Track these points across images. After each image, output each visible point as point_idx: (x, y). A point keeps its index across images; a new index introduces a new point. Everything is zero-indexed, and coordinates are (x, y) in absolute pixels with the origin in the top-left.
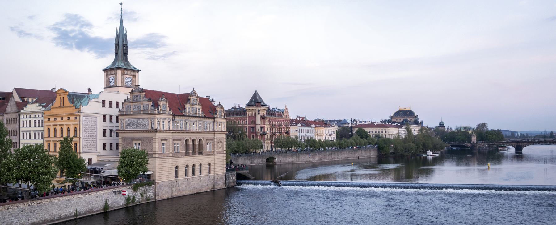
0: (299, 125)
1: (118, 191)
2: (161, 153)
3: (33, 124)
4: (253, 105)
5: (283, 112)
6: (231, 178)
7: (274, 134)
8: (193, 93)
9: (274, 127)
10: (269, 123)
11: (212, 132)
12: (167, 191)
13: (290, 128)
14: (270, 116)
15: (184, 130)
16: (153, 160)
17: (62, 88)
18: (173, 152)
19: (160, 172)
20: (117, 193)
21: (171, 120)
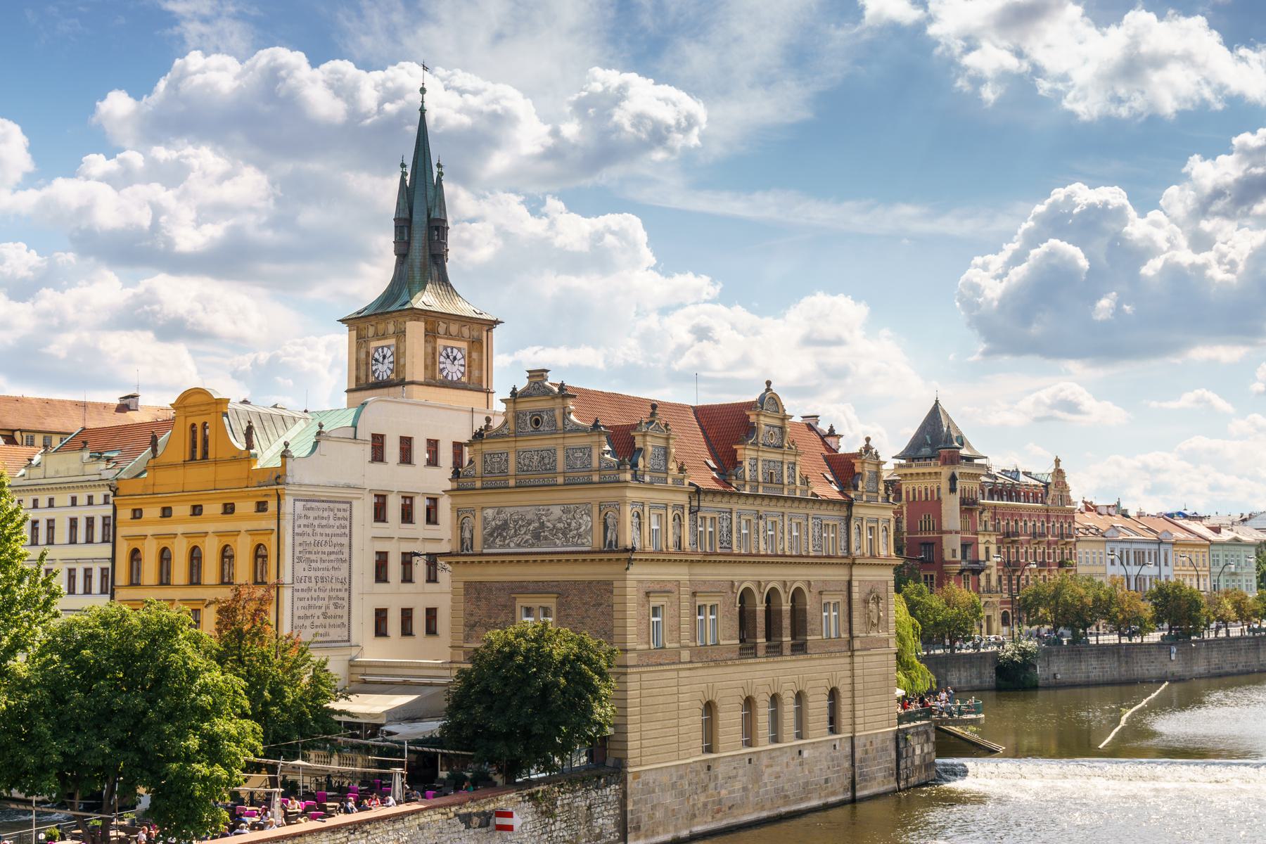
1: (477, 814)
2: (646, 647)
3: (62, 533)
4: (925, 459)
6: (918, 752)
7: (1011, 567)
8: (769, 401)
9: (1013, 542)
10: (994, 526)
11: (839, 561)
12: (674, 810)
13: (1078, 544)
14: (996, 497)
15: (736, 551)
17: (202, 387)
18: (693, 644)
19: (646, 726)
20: (476, 820)
21: (687, 512)
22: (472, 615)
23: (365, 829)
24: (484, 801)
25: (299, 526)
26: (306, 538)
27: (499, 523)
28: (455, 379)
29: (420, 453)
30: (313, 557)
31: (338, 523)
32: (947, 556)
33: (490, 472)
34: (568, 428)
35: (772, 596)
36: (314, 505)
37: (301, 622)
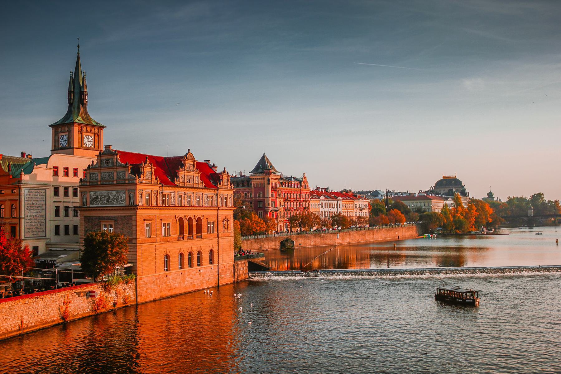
0: (322, 197)
1: (83, 292)
4: (260, 173)
5: (300, 182)
14: (283, 186)
16: (132, 247)
20: (82, 294)
21: (159, 193)
22: (86, 227)
23: (41, 297)
24: (85, 288)
25: (27, 198)
26: (29, 202)
27: (95, 197)
28: (89, 146)
29: (71, 172)
30: (32, 208)
31: (41, 197)
32: (266, 205)
33: (92, 180)
34: (118, 165)
35: (190, 219)
36: (32, 191)
37: (28, 230)
